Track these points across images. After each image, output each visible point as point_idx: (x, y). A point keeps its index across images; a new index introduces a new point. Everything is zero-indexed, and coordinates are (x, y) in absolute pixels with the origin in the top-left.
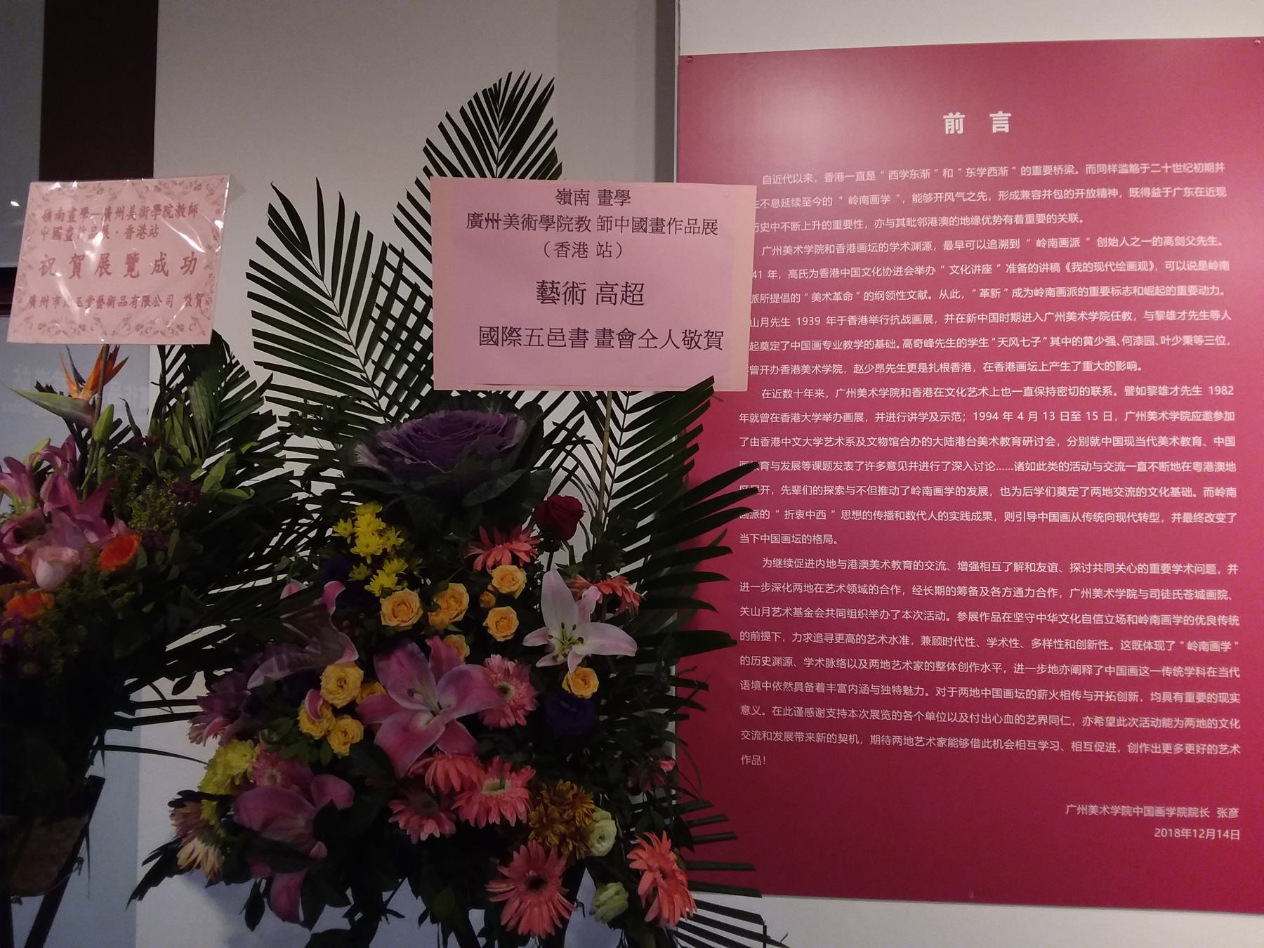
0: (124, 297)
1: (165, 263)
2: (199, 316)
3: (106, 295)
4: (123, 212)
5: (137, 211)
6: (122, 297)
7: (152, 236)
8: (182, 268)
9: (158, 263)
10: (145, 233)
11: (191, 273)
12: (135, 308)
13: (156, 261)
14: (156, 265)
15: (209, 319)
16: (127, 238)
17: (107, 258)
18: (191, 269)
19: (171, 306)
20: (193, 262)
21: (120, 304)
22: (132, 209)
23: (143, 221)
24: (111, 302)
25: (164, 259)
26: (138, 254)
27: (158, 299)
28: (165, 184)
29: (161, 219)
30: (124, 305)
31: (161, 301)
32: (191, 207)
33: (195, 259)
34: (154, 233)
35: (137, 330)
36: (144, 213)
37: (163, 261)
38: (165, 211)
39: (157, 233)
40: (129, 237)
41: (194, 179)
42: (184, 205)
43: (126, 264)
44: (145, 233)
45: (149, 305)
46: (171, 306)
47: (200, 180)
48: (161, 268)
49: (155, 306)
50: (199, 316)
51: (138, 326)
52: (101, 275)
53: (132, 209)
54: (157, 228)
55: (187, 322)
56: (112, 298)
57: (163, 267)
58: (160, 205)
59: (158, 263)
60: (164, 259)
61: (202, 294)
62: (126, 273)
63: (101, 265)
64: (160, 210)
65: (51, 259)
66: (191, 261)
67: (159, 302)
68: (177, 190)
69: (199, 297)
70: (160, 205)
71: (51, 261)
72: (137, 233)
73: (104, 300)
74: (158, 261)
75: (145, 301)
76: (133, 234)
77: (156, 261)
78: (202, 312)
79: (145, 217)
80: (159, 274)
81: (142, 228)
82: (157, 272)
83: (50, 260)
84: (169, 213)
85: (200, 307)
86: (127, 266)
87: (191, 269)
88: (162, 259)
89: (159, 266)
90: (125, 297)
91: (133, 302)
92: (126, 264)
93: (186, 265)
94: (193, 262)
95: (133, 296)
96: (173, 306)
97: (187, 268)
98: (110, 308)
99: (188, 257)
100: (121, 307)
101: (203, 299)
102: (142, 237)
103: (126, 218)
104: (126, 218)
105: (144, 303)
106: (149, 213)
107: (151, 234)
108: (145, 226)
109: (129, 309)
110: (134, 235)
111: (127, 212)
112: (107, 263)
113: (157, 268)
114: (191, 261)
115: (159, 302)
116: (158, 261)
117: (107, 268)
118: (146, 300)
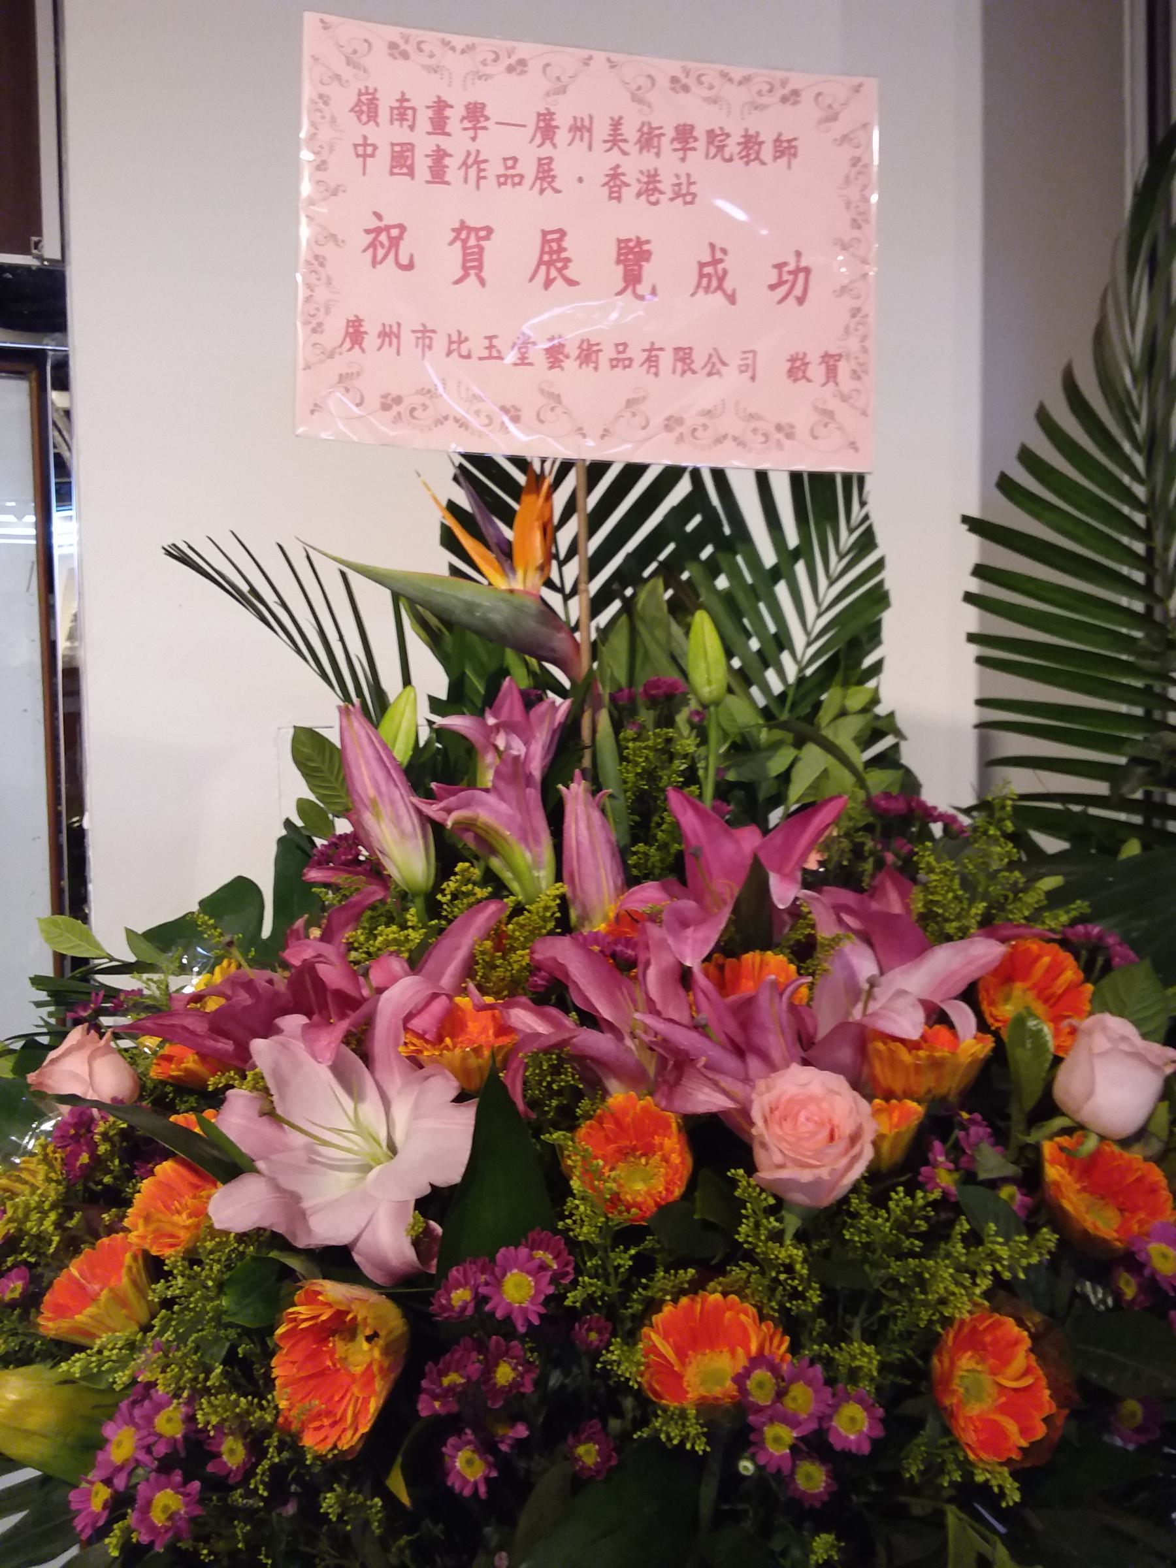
0: (622, 347)
2: (834, 404)
3: (572, 338)
4: (590, 130)
5: (630, 131)
6: (617, 345)
7: (680, 201)
8: (773, 287)
9: (707, 270)
10: (661, 193)
12: (656, 374)
14: (701, 275)
15: (864, 413)
16: (611, 198)
17: (559, 240)
18: (798, 291)
19: (753, 378)
21: (614, 363)
22: (616, 124)
23: (648, 161)
24: (588, 353)
26: (648, 242)
27: (715, 359)
28: (700, 76)
29: (697, 162)
30: (625, 367)
31: (724, 364)
32: (778, 140)
34: (685, 194)
35: (668, 428)
36: (649, 139)
37: (720, 267)
38: (710, 142)
39: (694, 195)
40: (615, 195)
41: (780, 75)
42: (758, 134)
43: (618, 262)
44: (661, 193)
45: (694, 372)
46: (753, 378)
47: (797, 81)
49: (710, 374)
50: (834, 404)
51: (668, 419)
53: (616, 124)
54: (690, 184)
55: (803, 419)
56: (590, 345)
57: (721, 280)
58: (692, 127)
59: (707, 270)
60: (721, 261)
61: (840, 355)
62: (621, 285)
63: (546, 258)
64: (696, 140)
66: (795, 273)
67: (719, 366)
68: (736, 95)
69: (830, 362)
70: (692, 127)
72: (635, 188)
73: (567, 350)
75: (683, 360)
76: (625, 190)
78: (844, 398)
79: (654, 150)
80: (710, 296)
81: (649, 176)
84: (721, 148)
85: (837, 384)
86: (621, 267)
87: (798, 291)
88: (715, 262)
90: (625, 345)
91: (648, 359)
92: (618, 262)
95: (648, 347)
96: (758, 375)
98: (588, 370)
100: (619, 370)
101: (844, 368)
102: (653, 199)
103: (599, 146)
104: (599, 146)
105: (679, 365)
106: (665, 141)
107: (677, 195)
108: (656, 175)
109: (638, 375)
110: (628, 193)
111: (602, 130)
112: (564, 255)
113: (705, 281)
115: (719, 366)
117: (565, 267)
118: (684, 356)
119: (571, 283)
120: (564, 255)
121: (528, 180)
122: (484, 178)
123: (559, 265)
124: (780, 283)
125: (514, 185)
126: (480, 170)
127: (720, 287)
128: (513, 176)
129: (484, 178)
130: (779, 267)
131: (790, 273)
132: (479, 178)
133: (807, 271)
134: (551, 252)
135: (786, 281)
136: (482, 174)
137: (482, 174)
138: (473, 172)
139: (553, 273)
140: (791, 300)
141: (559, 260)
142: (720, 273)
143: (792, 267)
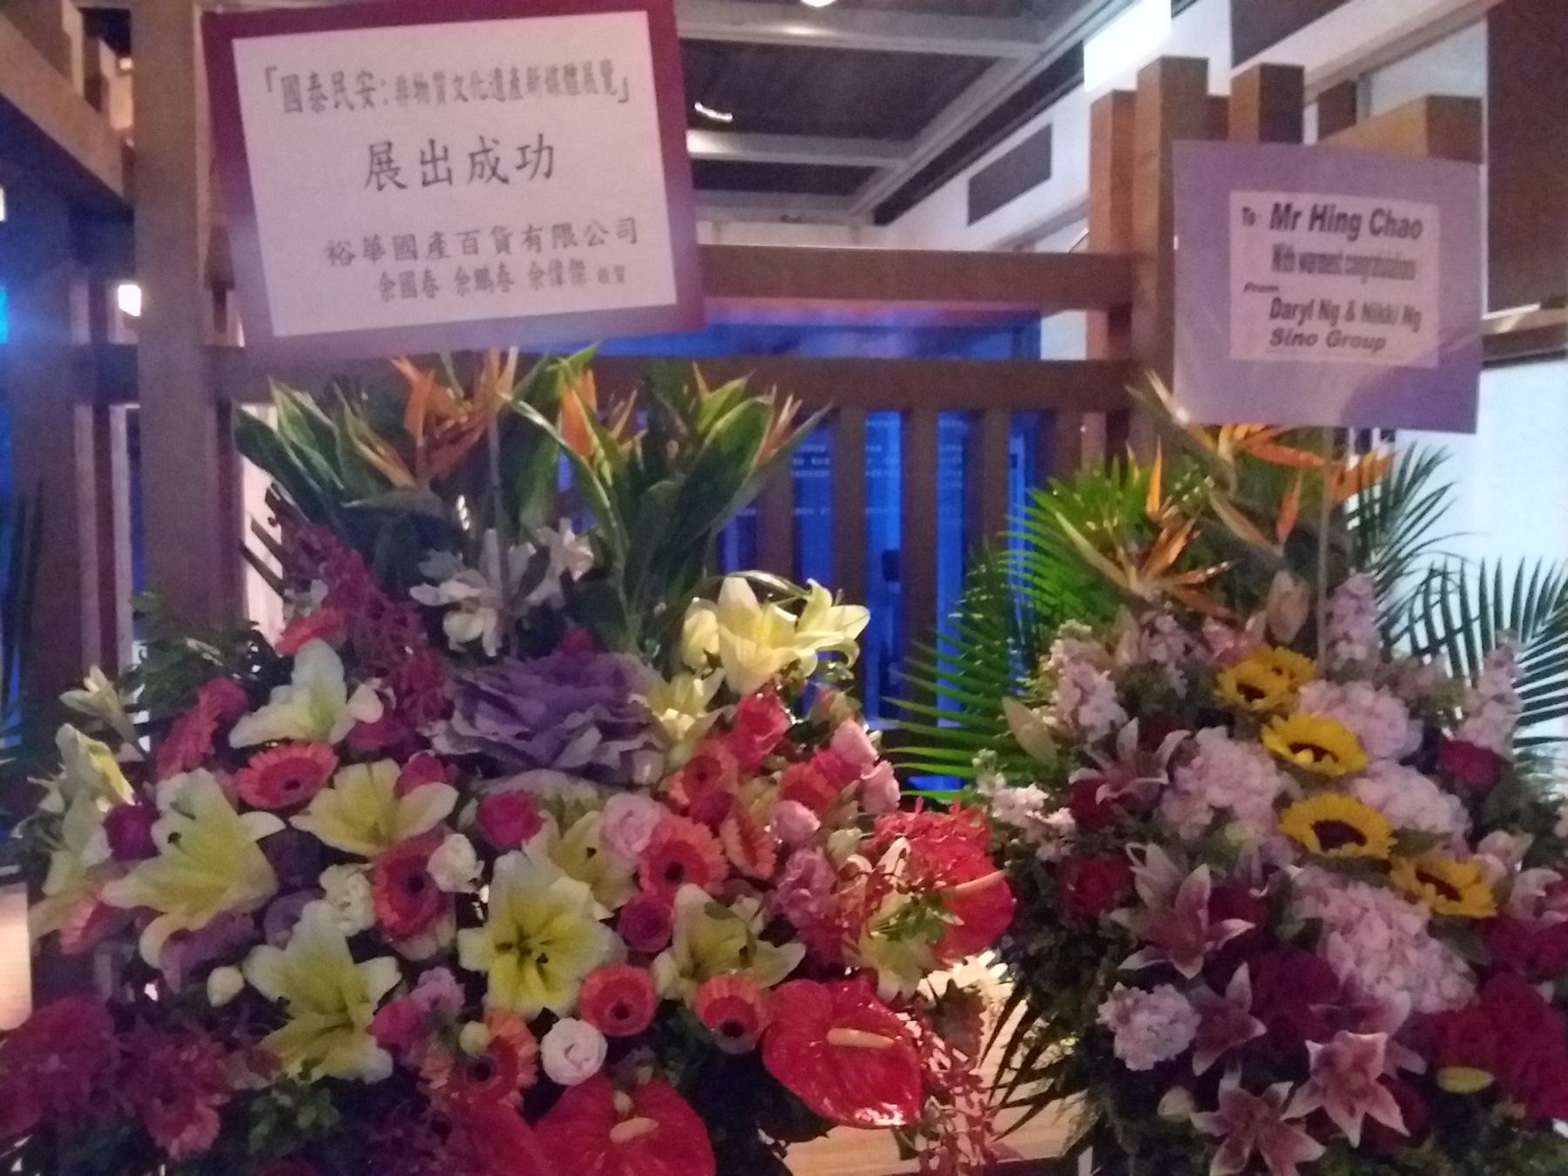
1: (497, 160)
11: (548, 175)
18: (544, 167)
37: (492, 156)
48: (488, 172)
59: (479, 158)
66: (539, 151)
77: (472, 155)
89: (482, 164)
94: (545, 154)
114: (539, 151)
119: (401, 186)
120: (393, 165)
123: (390, 174)
134: (380, 163)
139: (384, 179)
140: (540, 174)
141: (390, 169)
142: (493, 161)
143: (535, 146)
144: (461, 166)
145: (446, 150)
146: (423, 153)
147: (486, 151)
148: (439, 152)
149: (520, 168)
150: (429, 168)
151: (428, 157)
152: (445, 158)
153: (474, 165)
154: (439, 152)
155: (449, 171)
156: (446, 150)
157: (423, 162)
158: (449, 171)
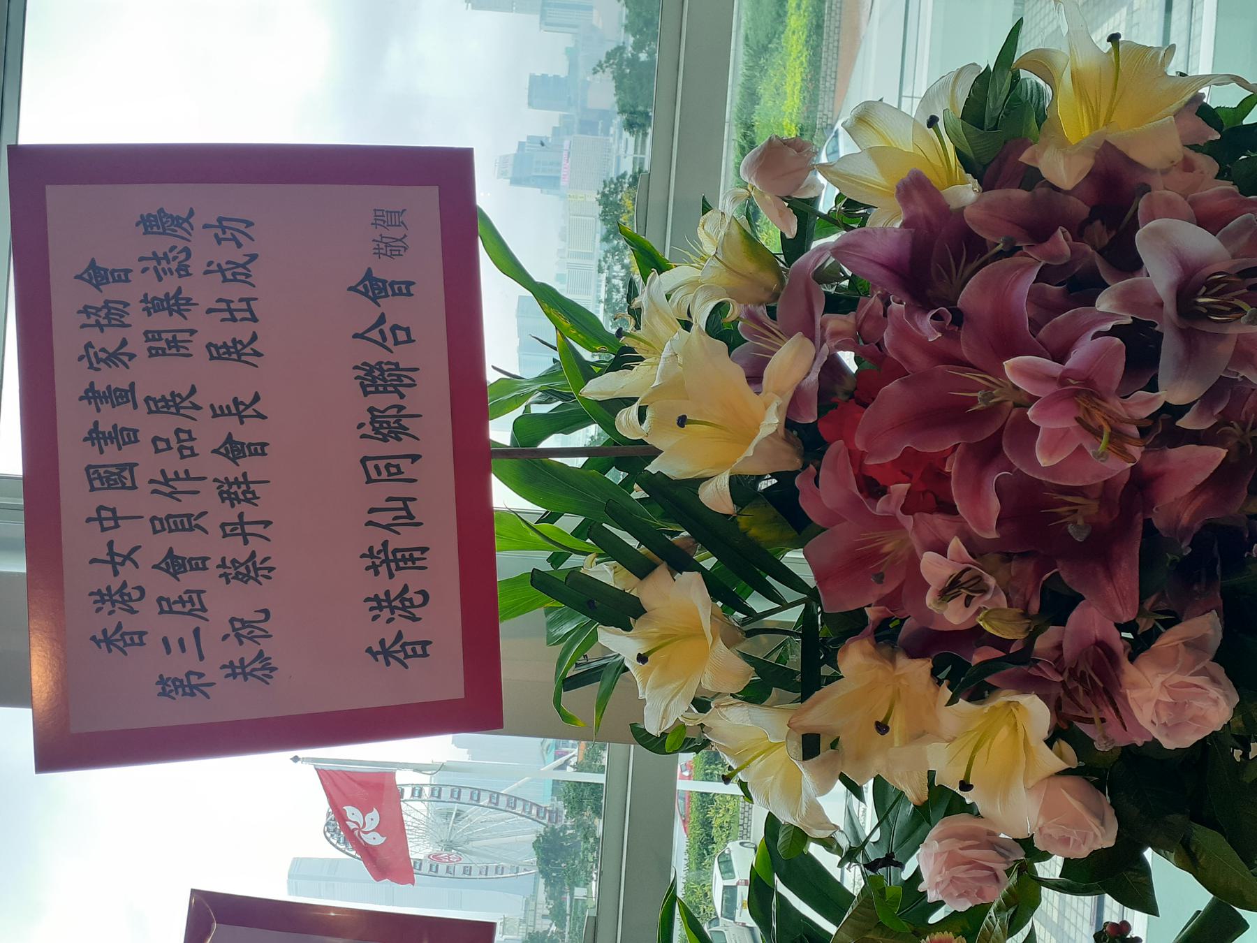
1: (228, 263)
13: (225, 280)
20: (225, 223)
25: (219, 265)
33: (220, 220)
37: (225, 266)
52: (257, 354)
57: (238, 266)
65: (233, 626)
71: (238, 625)
74: (224, 276)
77: (225, 280)
82: (248, 276)
83: (234, 629)
89: (234, 274)
93: (234, 239)
94: (225, 223)
97: (236, 234)
99: (216, 236)
116: (224, 276)
121: (185, 424)
122: (187, 472)
123: (239, 347)
124: (234, 239)
125: (191, 439)
126: (177, 478)
127: (244, 266)
128: (179, 441)
129: (187, 472)
130: (219, 241)
131: (224, 233)
132: (188, 478)
133: (220, 220)
134: (230, 354)
135: (232, 234)
136: (182, 475)
137: (182, 475)
138: (180, 486)
144: (235, 292)
145: (220, 300)
146: (223, 320)
147: (221, 270)
148: (223, 306)
149: (239, 245)
150: (238, 315)
151: (227, 315)
152: (228, 302)
153: (235, 280)
154: (223, 306)
155: (241, 300)
156: (220, 300)
157: (234, 320)
158: (241, 300)
